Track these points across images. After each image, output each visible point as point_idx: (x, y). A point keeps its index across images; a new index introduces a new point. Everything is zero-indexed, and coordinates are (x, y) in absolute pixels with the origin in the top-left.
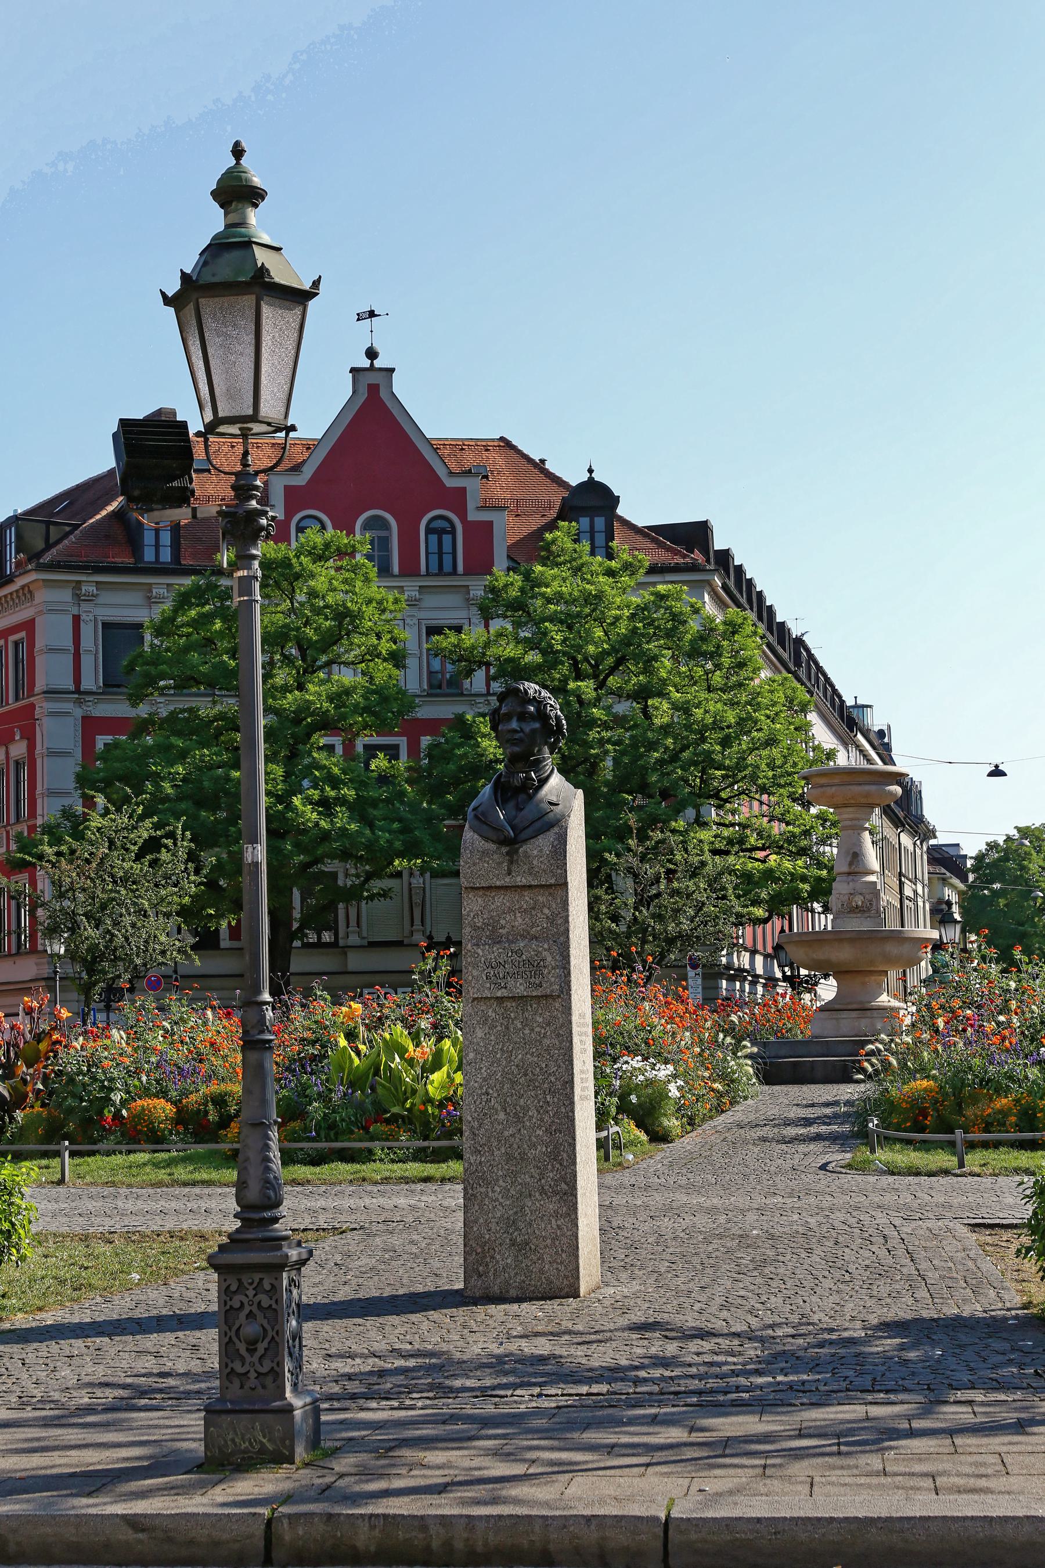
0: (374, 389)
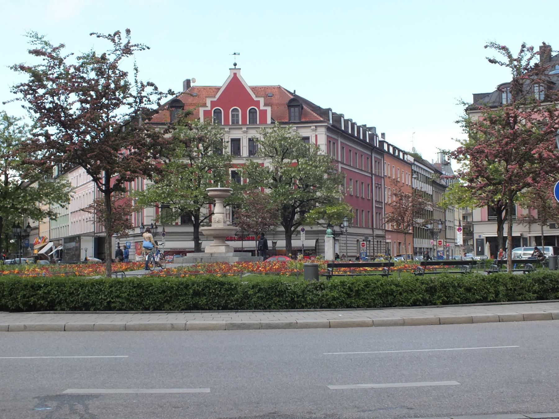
0: (235, 74)
